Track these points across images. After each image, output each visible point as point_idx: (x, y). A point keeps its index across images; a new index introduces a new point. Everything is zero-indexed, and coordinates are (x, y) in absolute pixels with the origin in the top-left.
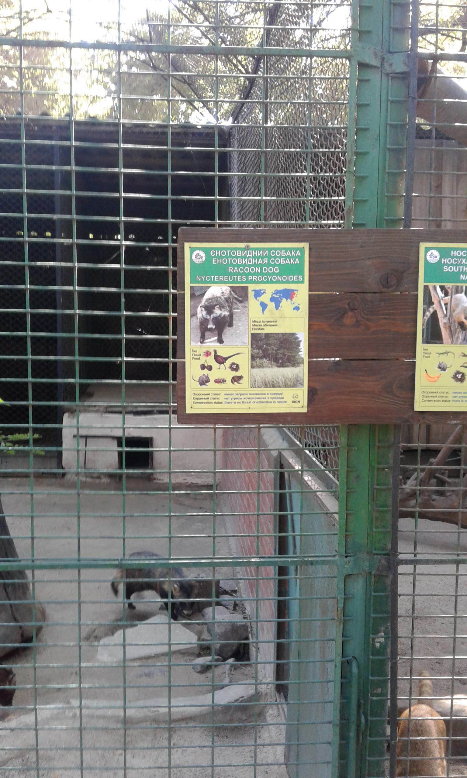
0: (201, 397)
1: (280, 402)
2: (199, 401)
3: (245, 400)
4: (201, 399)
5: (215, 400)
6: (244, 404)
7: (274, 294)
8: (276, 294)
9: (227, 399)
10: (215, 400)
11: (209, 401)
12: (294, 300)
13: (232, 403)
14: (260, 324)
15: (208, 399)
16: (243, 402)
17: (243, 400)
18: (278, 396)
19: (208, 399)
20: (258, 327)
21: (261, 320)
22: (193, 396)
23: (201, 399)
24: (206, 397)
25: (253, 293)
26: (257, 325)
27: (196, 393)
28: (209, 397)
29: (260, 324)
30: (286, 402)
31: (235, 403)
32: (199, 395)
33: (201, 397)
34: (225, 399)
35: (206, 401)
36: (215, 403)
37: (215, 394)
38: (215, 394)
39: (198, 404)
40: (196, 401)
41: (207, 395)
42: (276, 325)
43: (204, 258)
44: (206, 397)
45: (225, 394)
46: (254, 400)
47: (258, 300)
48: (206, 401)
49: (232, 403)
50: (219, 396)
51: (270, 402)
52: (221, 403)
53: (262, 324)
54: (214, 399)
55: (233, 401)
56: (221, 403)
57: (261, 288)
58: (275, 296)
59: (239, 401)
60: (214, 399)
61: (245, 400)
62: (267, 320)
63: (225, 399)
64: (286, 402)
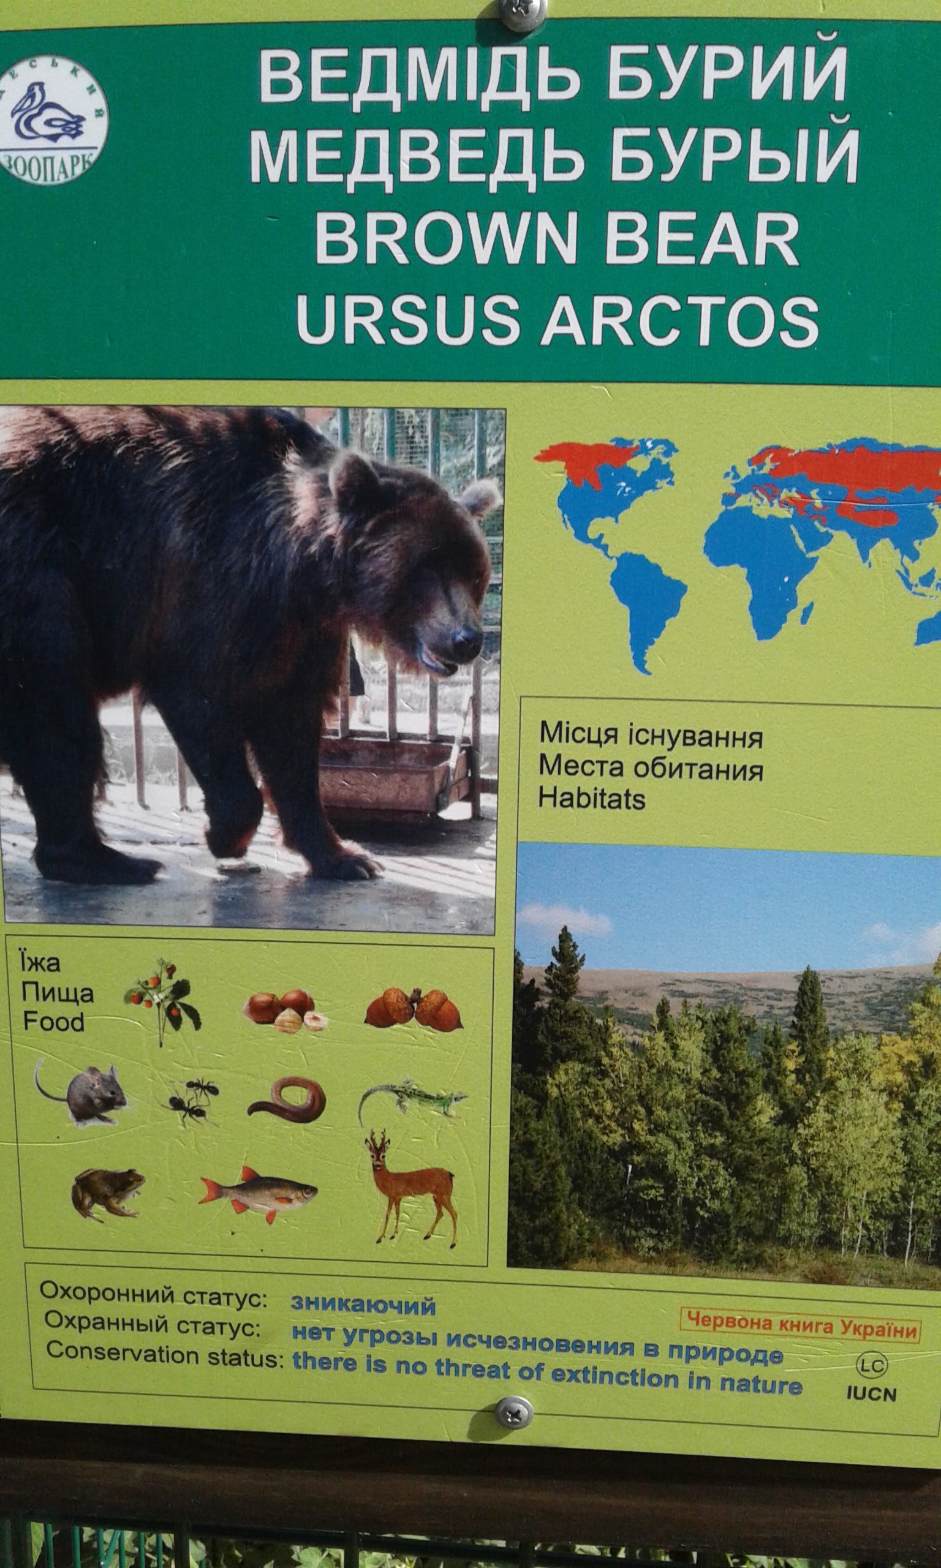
0: (101, 1308)
1: (744, 1385)
2: (93, 1338)
3: (461, 1355)
4: (100, 1323)
5: (219, 1342)
6: (451, 1382)
7: (745, 486)
8: (769, 487)
9: (315, 1333)
10: (219, 1342)
11: (171, 1340)
12: (924, 546)
13: (350, 1365)
14: (609, 752)
15: (162, 1325)
16: (445, 1367)
17: (442, 1351)
18: (735, 1339)
19: (162, 1325)
21: (620, 718)
23: (100, 1323)
24: (146, 1311)
25: (556, 474)
26: (572, 767)
28: (174, 1311)
29: (609, 752)
30: (796, 1388)
31: (380, 1366)
32: (90, 1294)
33: (101, 1308)
35: (152, 1340)
37: (216, 1299)
38: (216, 1299)
39: (85, 1363)
40: (70, 1336)
41: (149, 1296)
42: (757, 772)
43: (95, 133)
44: (146, 1311)
45: (300, 1303)
46: (530, 1358)
48: (152, 1340)
49: (350, 1365)
50: (248, 1314)
51: (671, 1379)
52: (271, 1361)
54: (210, 1328)
55: (359, 1351)
56: (271, 1361)
57: (633, 434)
58: (763, 508)
59: (413, 1353)
60: (210, 1328)
61: (461, 1355)
64: (796, 1388)
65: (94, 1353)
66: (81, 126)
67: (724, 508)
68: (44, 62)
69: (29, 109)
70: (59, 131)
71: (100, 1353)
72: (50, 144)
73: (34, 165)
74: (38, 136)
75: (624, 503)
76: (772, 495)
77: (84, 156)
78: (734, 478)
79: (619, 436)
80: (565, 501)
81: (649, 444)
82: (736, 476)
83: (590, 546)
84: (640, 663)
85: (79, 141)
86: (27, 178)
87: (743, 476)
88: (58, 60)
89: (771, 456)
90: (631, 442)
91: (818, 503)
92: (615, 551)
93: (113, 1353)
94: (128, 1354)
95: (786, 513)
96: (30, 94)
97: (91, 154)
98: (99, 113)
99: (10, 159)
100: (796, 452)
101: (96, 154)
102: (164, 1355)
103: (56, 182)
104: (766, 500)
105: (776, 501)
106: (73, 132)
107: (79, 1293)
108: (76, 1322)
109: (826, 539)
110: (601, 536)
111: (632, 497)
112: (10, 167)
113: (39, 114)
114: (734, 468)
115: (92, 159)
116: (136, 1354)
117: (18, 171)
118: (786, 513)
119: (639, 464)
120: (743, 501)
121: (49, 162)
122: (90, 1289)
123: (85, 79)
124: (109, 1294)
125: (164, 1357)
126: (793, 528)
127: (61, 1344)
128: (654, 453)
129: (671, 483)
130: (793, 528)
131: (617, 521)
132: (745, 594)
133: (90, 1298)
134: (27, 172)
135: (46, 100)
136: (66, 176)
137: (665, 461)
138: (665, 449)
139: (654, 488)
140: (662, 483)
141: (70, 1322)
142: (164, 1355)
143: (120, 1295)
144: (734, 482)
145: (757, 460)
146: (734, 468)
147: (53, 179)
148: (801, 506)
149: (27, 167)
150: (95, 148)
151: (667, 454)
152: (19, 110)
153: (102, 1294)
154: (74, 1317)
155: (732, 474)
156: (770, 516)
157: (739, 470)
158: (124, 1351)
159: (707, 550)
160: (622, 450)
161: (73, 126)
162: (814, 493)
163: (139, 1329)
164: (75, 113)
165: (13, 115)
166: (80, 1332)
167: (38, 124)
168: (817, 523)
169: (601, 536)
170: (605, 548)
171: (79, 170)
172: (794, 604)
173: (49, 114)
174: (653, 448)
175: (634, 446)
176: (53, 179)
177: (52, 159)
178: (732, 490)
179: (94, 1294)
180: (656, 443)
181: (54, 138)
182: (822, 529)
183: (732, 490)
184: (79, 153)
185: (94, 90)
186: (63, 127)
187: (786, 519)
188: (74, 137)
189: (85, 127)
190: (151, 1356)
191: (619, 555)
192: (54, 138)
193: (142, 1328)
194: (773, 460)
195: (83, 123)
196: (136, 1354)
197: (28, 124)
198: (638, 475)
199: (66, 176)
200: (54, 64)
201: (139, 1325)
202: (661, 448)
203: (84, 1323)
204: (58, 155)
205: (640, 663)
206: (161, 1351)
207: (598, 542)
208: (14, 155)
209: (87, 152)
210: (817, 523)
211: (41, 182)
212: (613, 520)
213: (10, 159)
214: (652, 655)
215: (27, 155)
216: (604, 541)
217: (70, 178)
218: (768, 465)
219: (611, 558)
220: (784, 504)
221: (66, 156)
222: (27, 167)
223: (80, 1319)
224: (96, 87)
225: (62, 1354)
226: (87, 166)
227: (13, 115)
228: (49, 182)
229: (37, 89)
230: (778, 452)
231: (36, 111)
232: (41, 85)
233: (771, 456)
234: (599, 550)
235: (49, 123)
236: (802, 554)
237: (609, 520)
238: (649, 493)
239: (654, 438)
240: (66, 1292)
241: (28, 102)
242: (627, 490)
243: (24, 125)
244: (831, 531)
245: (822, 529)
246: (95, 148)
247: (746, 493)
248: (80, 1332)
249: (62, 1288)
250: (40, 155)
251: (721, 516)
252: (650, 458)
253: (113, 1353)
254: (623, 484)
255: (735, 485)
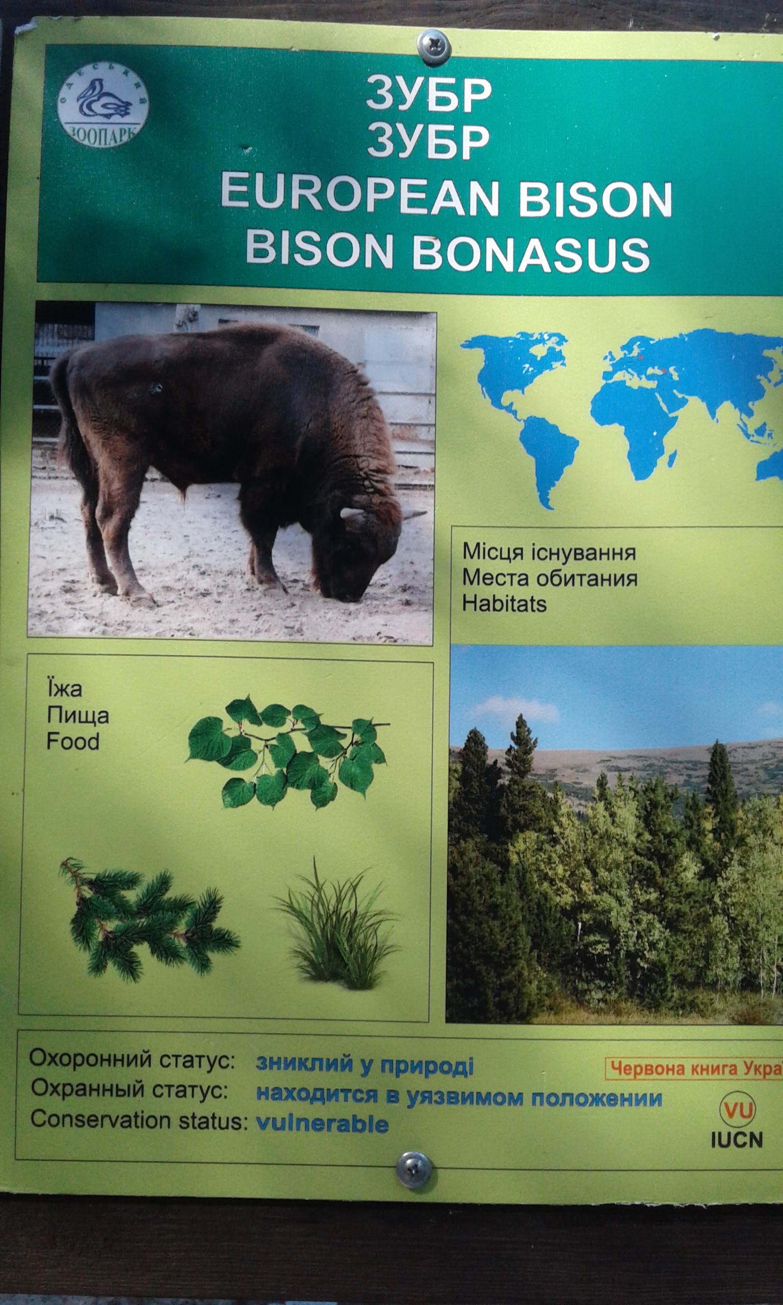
4: (83, 1090)
7: (619, 366)
8: (638, 365)
15: (137, 1090)
19: (137, 1090)
20: (502, 592)
22: (30, 1072)
23: (83, 1090)
27: (54, 1045)
34: (261, 1093)
36: (184, 1123)
39: (68, 1132)
40: (54, 1104)
47: (509, 409)
53: (527, 565)
57: (534, 328)
58: (634, 382)
62: (568, 542)
63: (261, 1093)
65: (74, 1121)
66: (129, 109)
67: (604, 382)
68: (103, 66)
69: (90, 96)
70: (112, 111)
71: (81, 1121)
72: (105, 120)
73: (92, 133)
74: (96, 114)
75: (527, 380)
76: (640, 372)
77: (130, 129)
78: (610, 360)
79: (523, 330)
80: (484, 378)
81: (546, 337)
82: (613, 358)
83: (504, 411)
84: (544, 500)
85: (127, 119)
86: (86, 142)
87: (617, 359)
88: (114, 65)
89: (639, 343)
90: (532, 336)
91: (676, 377)
92: (523, 415)
93: (93, 1121)
94: (106, 1121)
95: (652, 385)
96: (92, 86)
97: (135, 128)
98: (142, 101)
99: (74, 129)
100: (657, 340)
101: (139, 128)
102: (139, 1120)
103: (108, 146)
104: (636, 375)
105: (643, 377)
106: (123, 113)
107: (65, 1059)
108: (60, 1089)
109: (684, 402)
110: (512, 404)
111: (534, 375)
112: (74, 135)
113: (98, 100)
114: (610, 353)
115: (136, 132)
116: (114, 1120)
117: (80, 138)
118: (652, 385)
119: (539, 351)
120: (619, 376)
121: (103, 133)
122: (75, 1055)
123: (133, 77)
124: (92, 1060)
125: (139, 1124)
126: (656, 394)
127: (44, 1113)
128: (550, 344)
129: (563, 364)
130: (656, 394)
131: (523, 393)
132: (624, 445)
133: (75, 1064)
134: (87, 139)
135: (104, 91)
136: (116, 141)
137: (558, 348)
138: (558, 340)
139: (551, 368)
140: (556, 365)
141: (55, 1089)
142: (139, 1120)
143: (102, 1060)
144: (611, 363)
145: (628, 347)
146: (610, 353)
147: (106, 144)
148: (665, 383)
149: (87, 135)
150: (139, 124)
151: (559, 344)
152: (82, 97)
153: (85, 1060)
154: (58, 1085)
155: (609, 357)
156: (641, 389)
157: (614, 354)
158: (103, 1117)
159: (594, 413)
160: (526, 341)
161: (123, 109)
162: (671, 369)
163: (117, 1095)
164: (124, 100)
165: (78, 100)
166: (64, 1099)
167: (97, 107)
168: (675, 391)
169: (512, 404)
170: (515, 413)
171: (125, 138)
172: (661, 452)
173: (105, 100)
174: (549, 339)
175: (535, 338)
176: (106, 144)
177: (106, 130)
178: (610, 369)
179: (79, 1060)
180: (551, 336)
181: (108, 116)
182: (680, 396)
183: (610, 369)
184: (126, 127)
185: (140, 86)
186: (116, 109)
187: (652, 391)
188: (122, 116)
189: (132, 109)
190: (127, 1121)
191: (526, 419)
192: (108, 116)
193: (121, 1093)
194: (639, 347)
195: (131, 107)
196: (114, 1120)
197: (89, 107)
198: (539, 359)
199: (116, 141)
200: (111, 68)
201: (118, 1090)
202: (554, 339)
203: (68, 1090)
204: (110, 128)
205: (544, 500)
206: (136, 1116)
207: (509, 409)
208: (77, 127)
209: (132, 127)
210: (675, 391)
211: (97, 145)
212: (521, 391)
213: (74, 129)
214: (553, 493)
215: (87, 128)
216: (514, 408)
217: (119, 143)
218: (636, 352)
219: (520, 421)
220: (650, 378)
221: (117, 129)
222: (87, 135)
223: (64, 1085)
224: (141, 83)
225: (45, 1122)
226: (132, 136)
227: (78, 100)
228: (103, 146)
229: (97, 83)
230: (644, 341)
231: (96, 98)
232: (100, 81)
233: (639, 343)
234: (511, 415)
235: (104, 106)
236: (666, 415)
237: (517, 392)
238: (546, 372)
239: (549, 332)
240: (53, 1059)
241: (90, 92)
242: (531, 369)
243: (86, 107)
244: (687, 397)
245: (680, 396)
246: (139, 124)
247: (621, 370)
248: (64, 1099)
249: (50, 1055)
250: (97, 127)
251: (602, 388)
252: (547, 347)
253: (93, 1121)
254: (527, 366)
255: (612, 365)
